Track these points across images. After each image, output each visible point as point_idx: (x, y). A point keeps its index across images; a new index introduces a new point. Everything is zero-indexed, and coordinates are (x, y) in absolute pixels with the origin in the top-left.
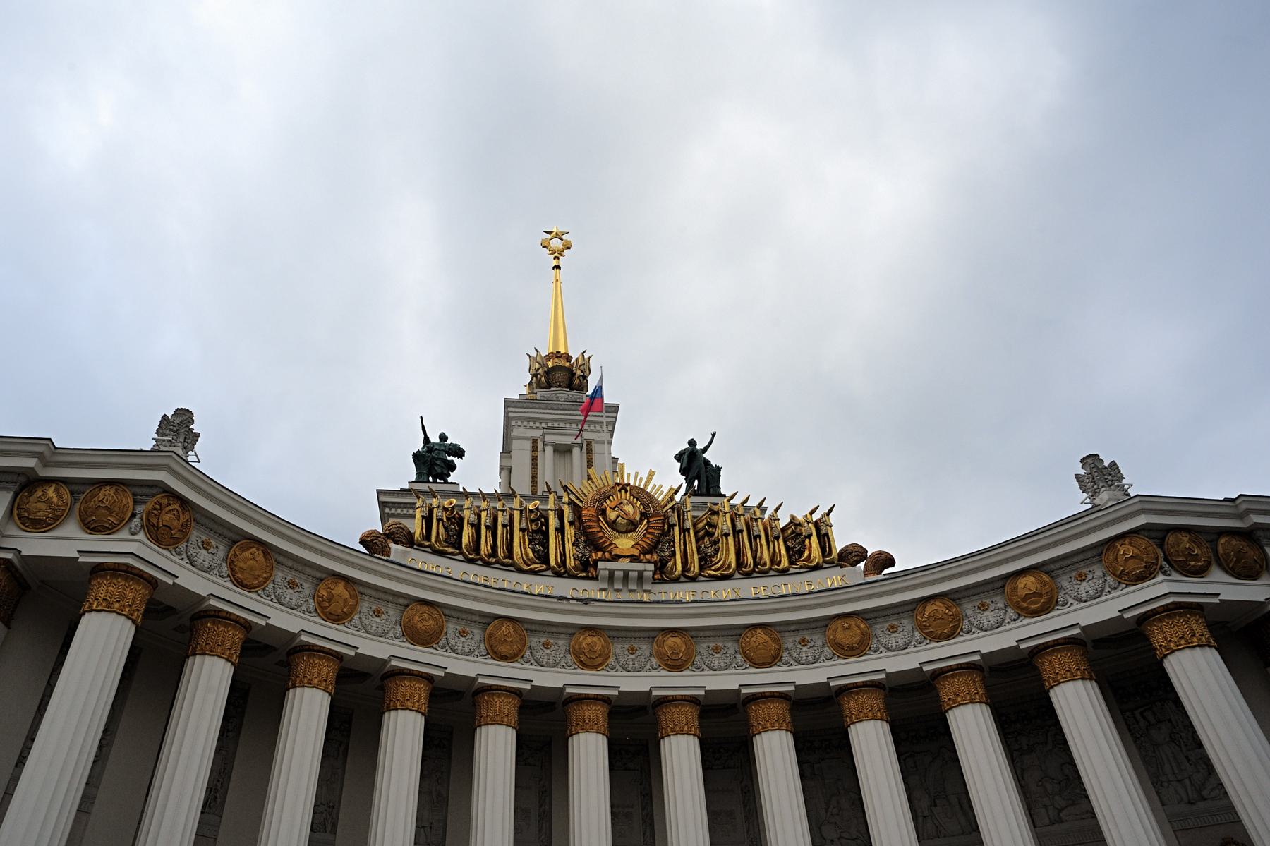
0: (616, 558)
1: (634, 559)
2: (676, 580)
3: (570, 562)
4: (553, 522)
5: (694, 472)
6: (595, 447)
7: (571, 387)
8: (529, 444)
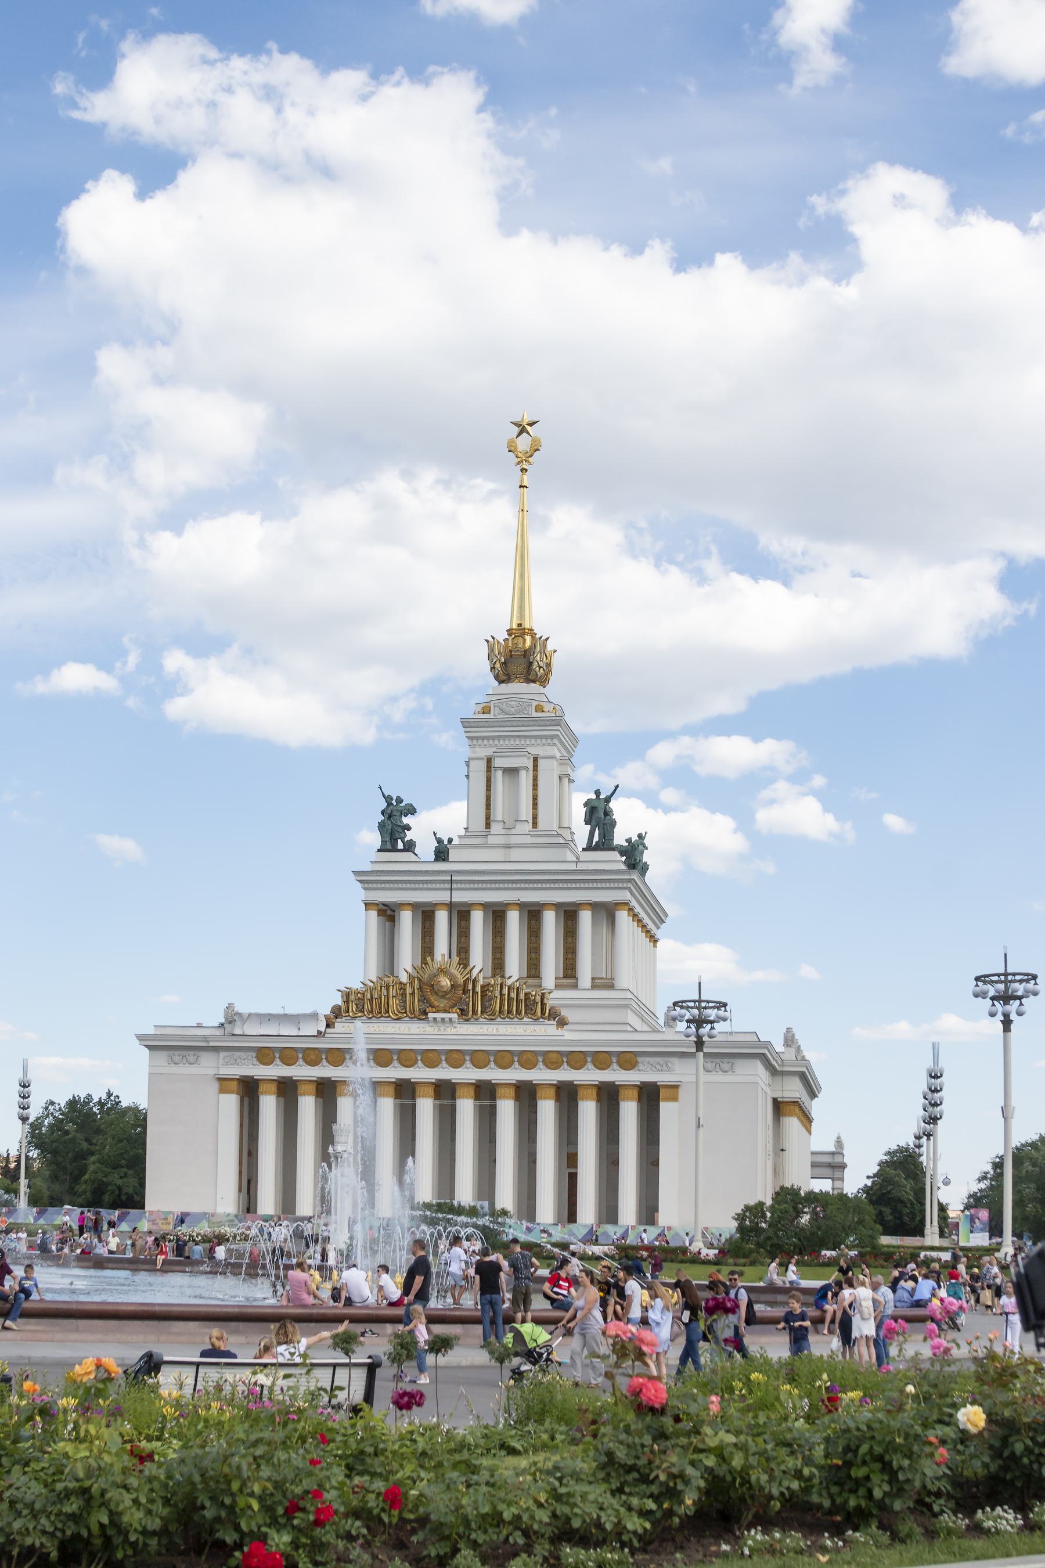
0: (438, 1011)
1: (445, 1011)
2: (467, 1020)
3: (417, 1013)
4: (409, 990)
5: (593, 823)
6: (541, 763)
7: (530, 677)
8: (483, 765)
